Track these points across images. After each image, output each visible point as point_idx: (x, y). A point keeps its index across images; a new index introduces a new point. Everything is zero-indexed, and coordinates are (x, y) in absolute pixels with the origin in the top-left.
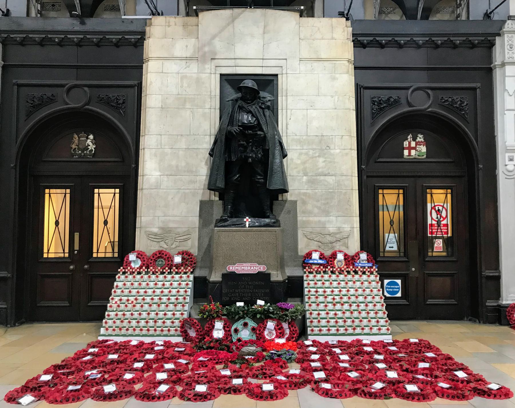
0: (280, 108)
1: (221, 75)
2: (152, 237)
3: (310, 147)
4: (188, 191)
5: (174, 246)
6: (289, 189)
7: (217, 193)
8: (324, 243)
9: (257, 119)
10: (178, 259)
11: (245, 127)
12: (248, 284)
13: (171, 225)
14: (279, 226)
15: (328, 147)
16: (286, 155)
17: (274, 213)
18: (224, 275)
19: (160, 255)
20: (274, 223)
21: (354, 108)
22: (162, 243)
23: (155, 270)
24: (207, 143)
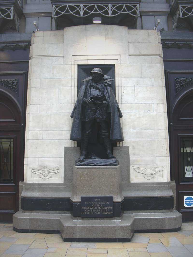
0: (117, 85)
1: (78, 65)
3: (137, 111)
4: (57, 141)
6: (124, 139)
7: (76, 142)
8: (147, 175)
9: (103, 93)
11: (95, 98)
12: (98, 204)
13: (46, 163)
14: (118, 165)
15: (149, 110)
16: (122, 116)
17: (114, 155)
18: (82, 198)
20: (115, 162)
21: (165, 86)
24: (70, 109)
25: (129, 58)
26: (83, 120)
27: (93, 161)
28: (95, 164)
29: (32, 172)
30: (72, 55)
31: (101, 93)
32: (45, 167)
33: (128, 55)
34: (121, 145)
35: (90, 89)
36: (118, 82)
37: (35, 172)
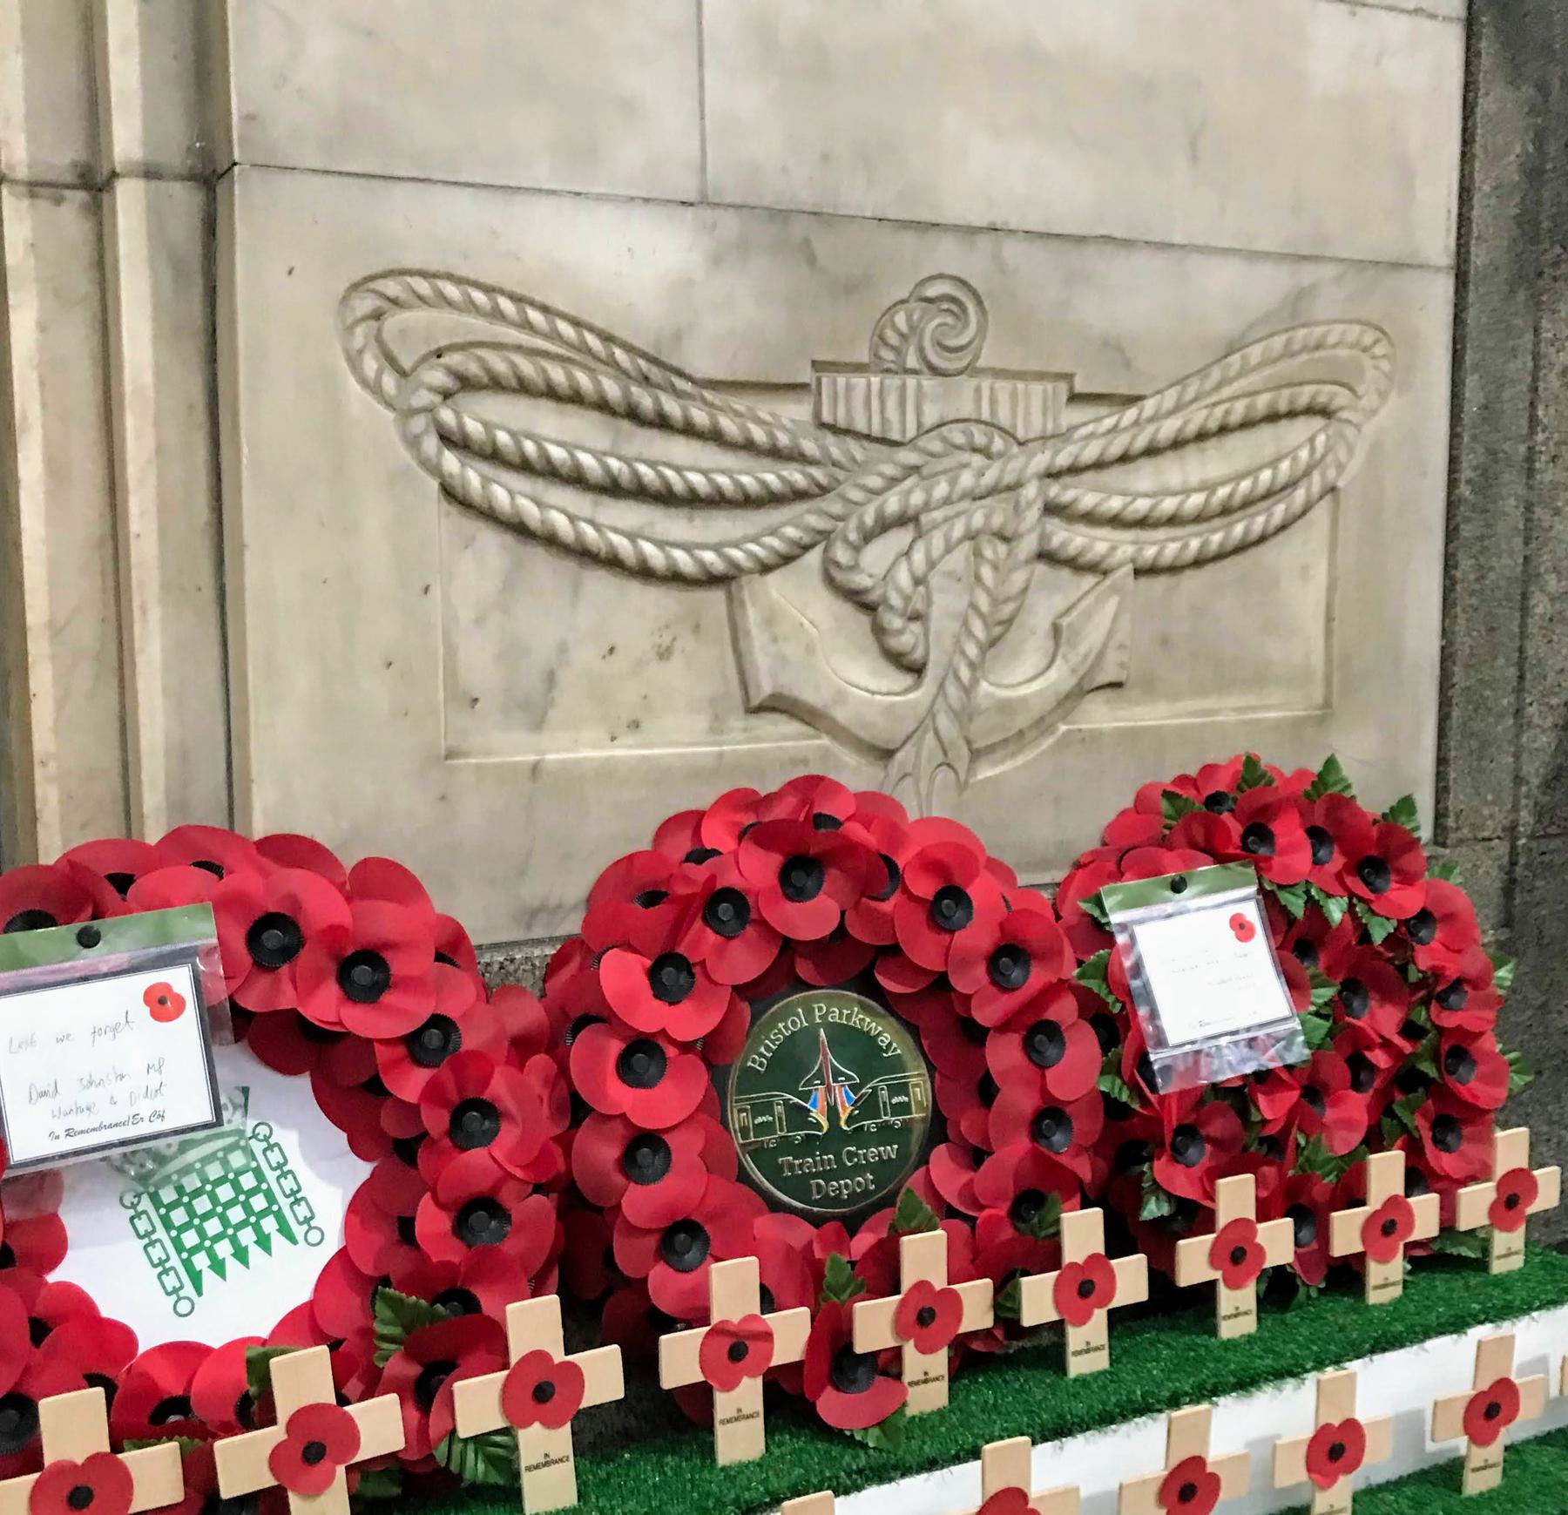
2: (555, 438)
5: (1026, 678)
10: (1210, 978)
13: (991, 167)
19: (814, 917)
22: (797, 603)
23: (832, 1335)
29: (451, 494)
32: (944, 321)
37: (561, 511)
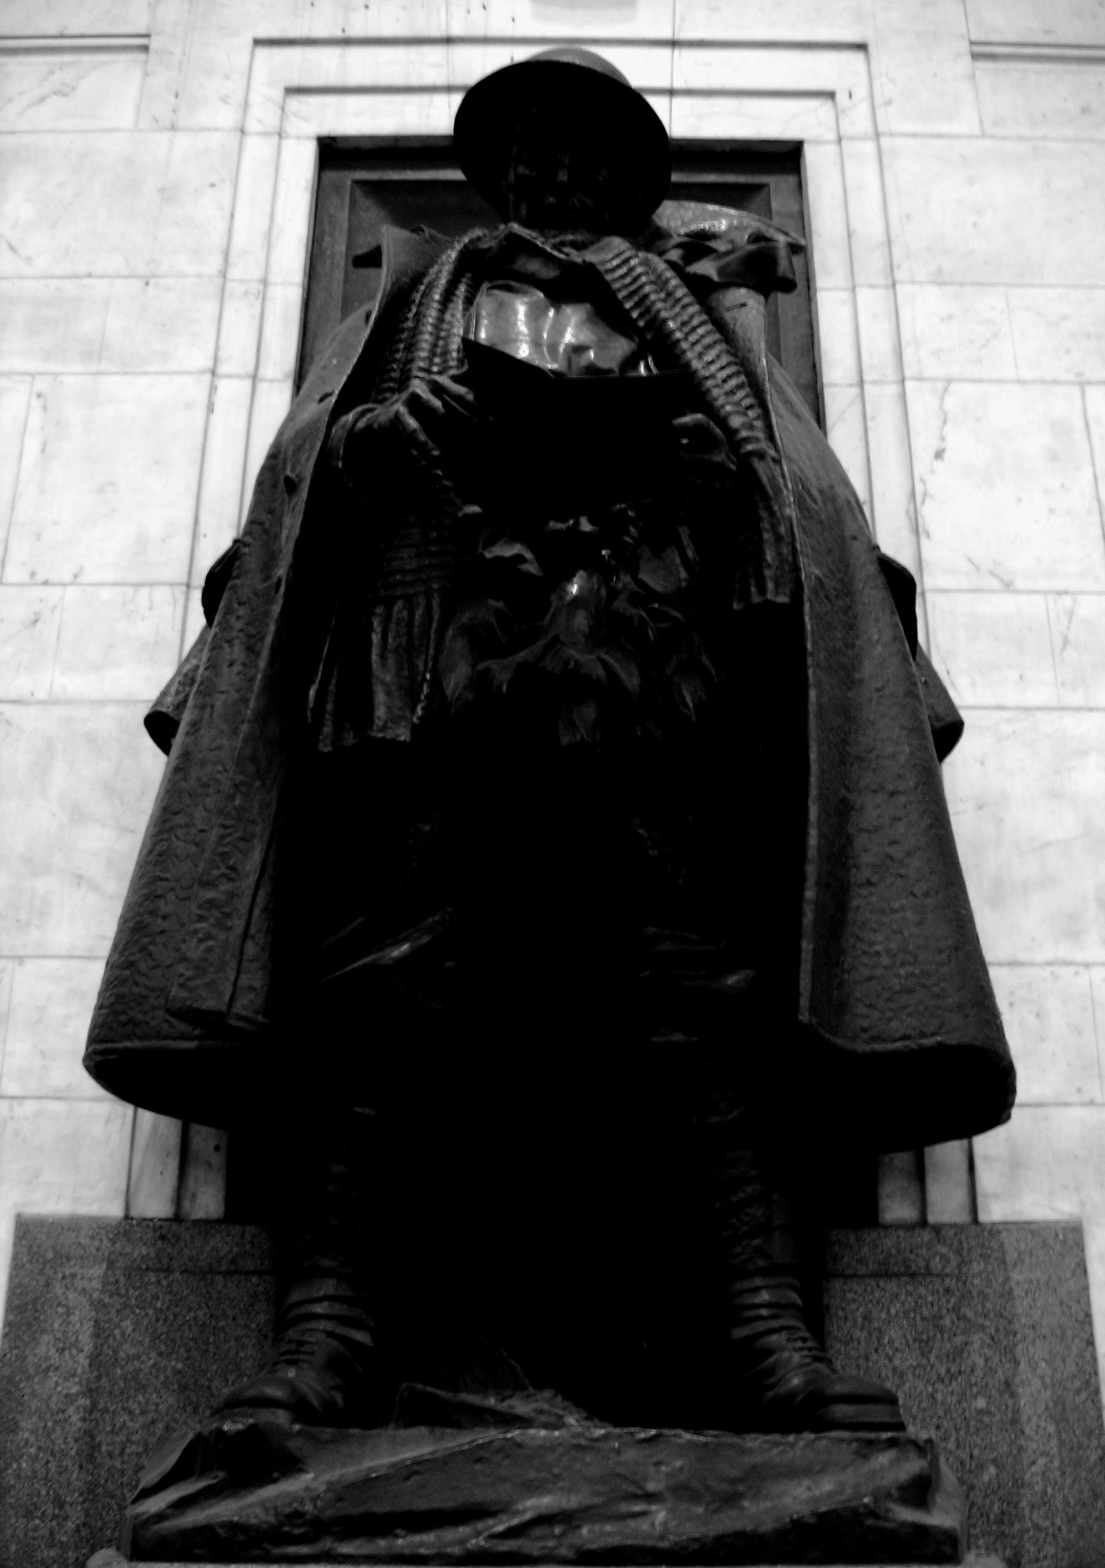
9: (654, 340)
25: (973, 77)
26: (326, 748)
27: (477, 1455)
28: (511, 1533)
30: (258, 42)
31: (621, 347)
33: (965, 47)
34: (946, 1203)
35: (469, 301)
36: (845, 319)
